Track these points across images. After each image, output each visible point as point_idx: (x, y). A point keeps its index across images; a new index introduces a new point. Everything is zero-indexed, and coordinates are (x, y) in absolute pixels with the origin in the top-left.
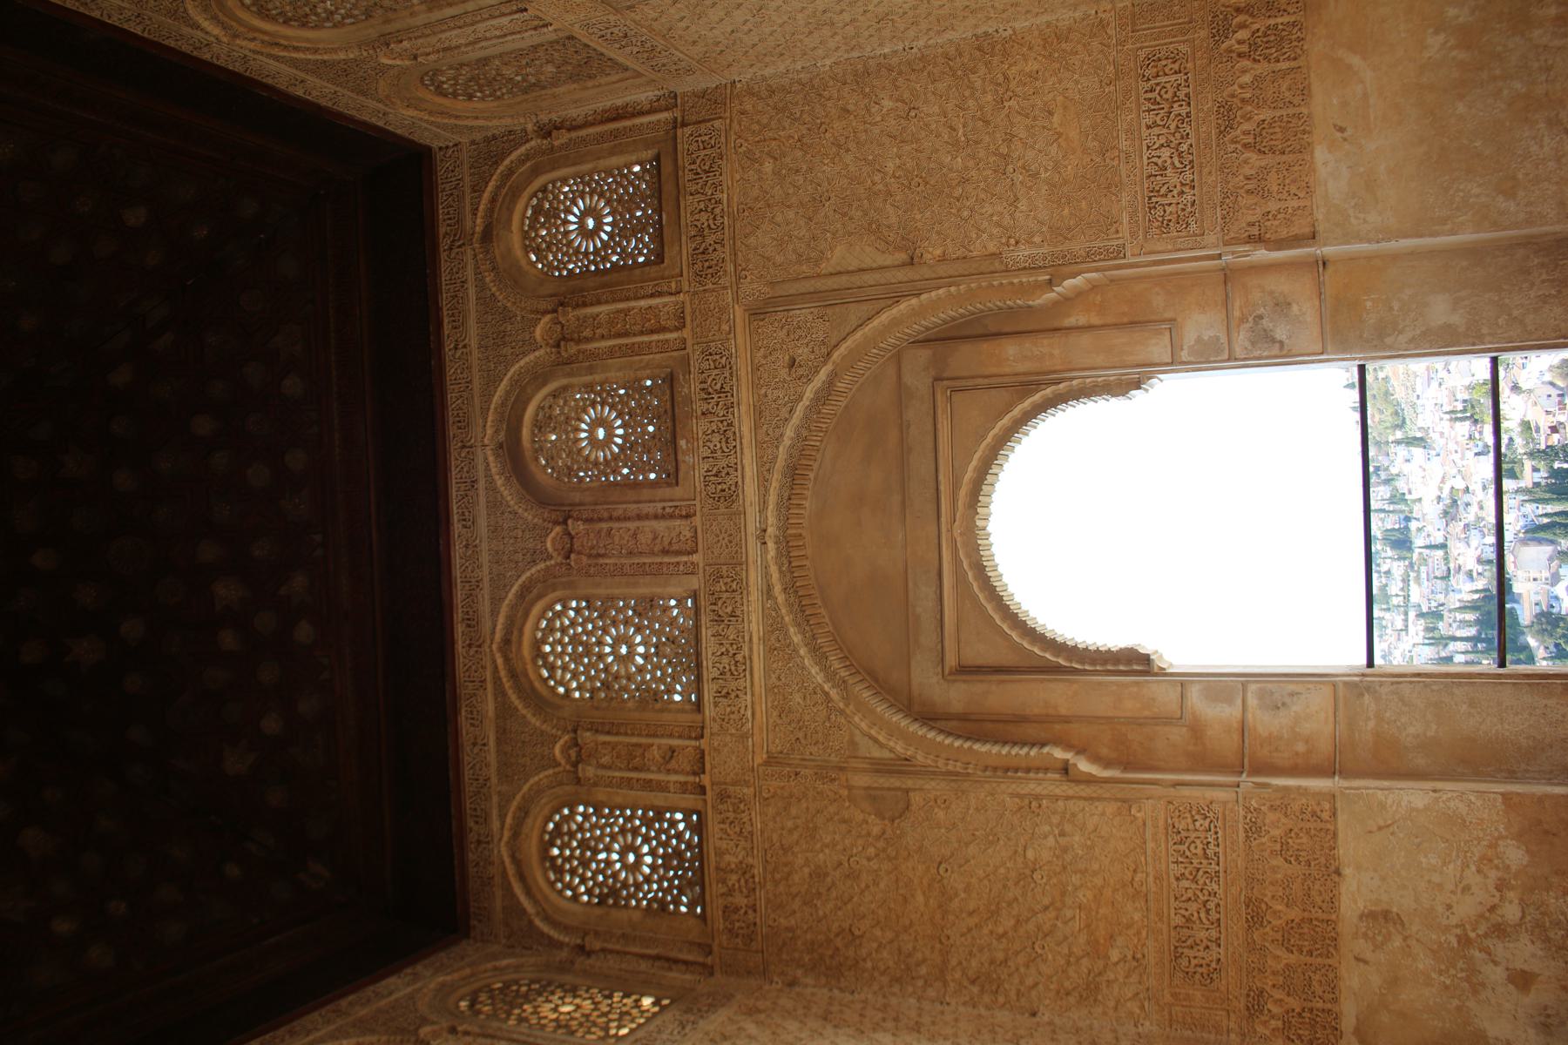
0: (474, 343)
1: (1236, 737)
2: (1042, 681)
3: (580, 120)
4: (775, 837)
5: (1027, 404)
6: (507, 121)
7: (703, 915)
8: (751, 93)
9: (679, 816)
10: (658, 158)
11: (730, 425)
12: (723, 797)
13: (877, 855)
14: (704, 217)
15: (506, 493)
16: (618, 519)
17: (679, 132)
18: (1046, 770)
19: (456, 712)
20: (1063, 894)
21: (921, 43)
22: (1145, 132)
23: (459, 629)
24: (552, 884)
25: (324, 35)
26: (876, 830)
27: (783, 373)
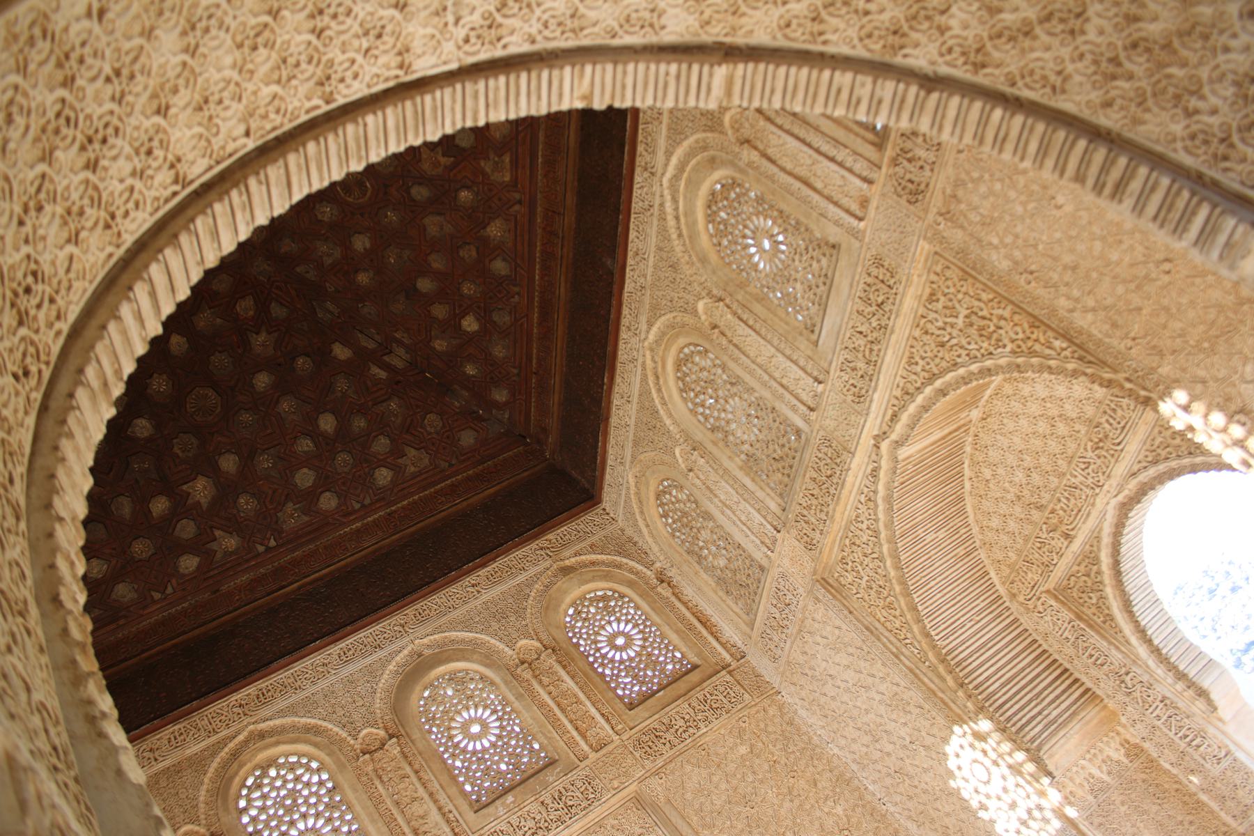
0: (485, 597)
3: (685, 599)
6: (655, 549)
10: (695, 667)
11: (549, 830)
14: (681, 723)
15: (385, 676)
16: (420, 779)
17: (724, 672)
19: (175, 721)
21: (892, 809)
23: (251, 690)
25: (680, 407)
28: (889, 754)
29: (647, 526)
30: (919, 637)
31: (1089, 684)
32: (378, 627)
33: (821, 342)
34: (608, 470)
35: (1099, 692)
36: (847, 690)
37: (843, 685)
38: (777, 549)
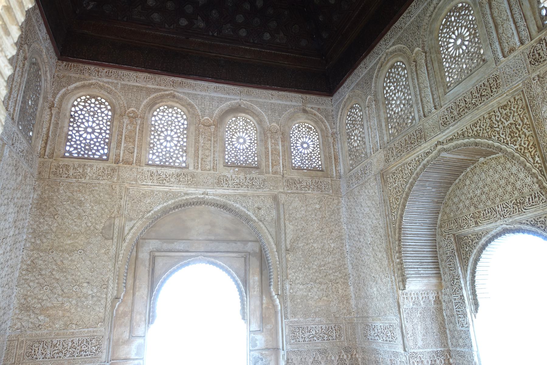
0: (272, 101)
1: (124, 357)
2: (148, 286)
4: (97, 188)
5: (239, 282)
7: (64, 157)
8: (339, 203)
9: (106, 151)
11: (242, 186)
12: (113, 170)
13: (88, 226)
16: (214, 144)
18: (118, 290)
19: (150, 73)
20: (69, 297)
21: (349, 257)
22: (320, 326)
23: (180, 79)
24: (80, 97)
26: (98, 227)
27: (256, 205)
28: (360, 242)
29: (341, 115)
30: (398, 216)
31: (442, 272)
32: (233, 87)
33: (448, 94)
34: (342, 87)
35: (442, 277)
36: (363, 213)
37: (363, 211)
38: (376, 154)
